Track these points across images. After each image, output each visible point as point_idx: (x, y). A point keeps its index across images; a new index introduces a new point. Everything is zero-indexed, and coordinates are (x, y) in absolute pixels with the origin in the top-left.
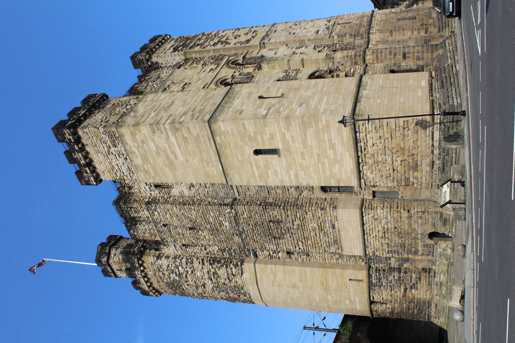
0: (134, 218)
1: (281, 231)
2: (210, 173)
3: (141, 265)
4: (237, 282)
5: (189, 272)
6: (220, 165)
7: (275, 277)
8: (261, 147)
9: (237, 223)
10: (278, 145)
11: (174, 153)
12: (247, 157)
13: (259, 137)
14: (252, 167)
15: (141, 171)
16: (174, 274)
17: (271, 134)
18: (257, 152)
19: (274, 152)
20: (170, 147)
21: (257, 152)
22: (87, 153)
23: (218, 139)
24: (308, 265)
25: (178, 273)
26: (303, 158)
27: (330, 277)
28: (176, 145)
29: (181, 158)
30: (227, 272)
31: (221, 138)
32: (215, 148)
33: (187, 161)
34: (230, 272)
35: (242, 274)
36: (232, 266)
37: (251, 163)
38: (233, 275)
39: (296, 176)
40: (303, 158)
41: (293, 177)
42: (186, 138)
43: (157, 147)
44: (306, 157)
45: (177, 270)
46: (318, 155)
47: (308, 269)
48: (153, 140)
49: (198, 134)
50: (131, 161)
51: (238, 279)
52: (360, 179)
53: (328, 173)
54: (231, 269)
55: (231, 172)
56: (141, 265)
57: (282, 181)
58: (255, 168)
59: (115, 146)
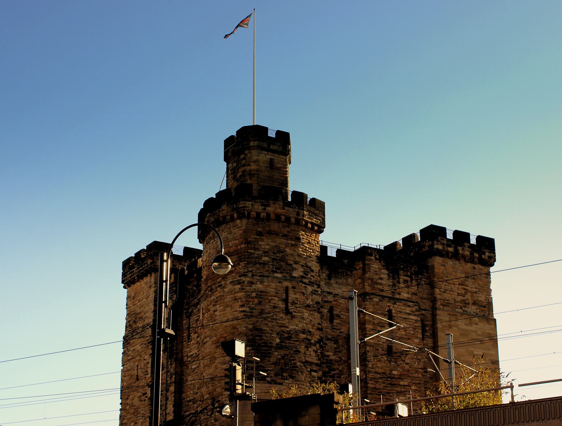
0: (398, 275)
4: (302, 372)
16: (302, 274)
25: (304, 280)
34: (315, 368)
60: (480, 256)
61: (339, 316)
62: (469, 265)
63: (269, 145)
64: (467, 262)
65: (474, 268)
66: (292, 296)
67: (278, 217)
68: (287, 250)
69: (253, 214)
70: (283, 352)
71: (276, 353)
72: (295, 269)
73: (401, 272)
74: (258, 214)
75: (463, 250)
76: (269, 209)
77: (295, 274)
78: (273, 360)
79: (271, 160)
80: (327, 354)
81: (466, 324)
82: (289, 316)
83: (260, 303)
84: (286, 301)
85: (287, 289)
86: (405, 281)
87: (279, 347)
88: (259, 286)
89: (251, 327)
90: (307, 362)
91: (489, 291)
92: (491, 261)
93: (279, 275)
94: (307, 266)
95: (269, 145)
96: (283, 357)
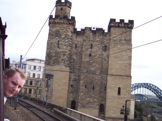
0: (96, 34)
1: (89, 88)
2: (113, 70)
3: (69, 23)
4: (61, 63)
5: (65, 44)
6: (115, 74)
7: (64, 79)
8: (121, 90)
9: (93, 73)
10: (122, 95)
11: (121, 60)
12: (118, 85)
13: (125, 90)
14: (115, 85)
15: (115, 45)
16: (64, 37)
17: (126, 94)
18: (119, 88)
19: (119, 93)
20: (123, 60)
21: (119, 88)
22: (123, 28)
23: (125, 77)
24: (68, 92)
25: (65, 38)
26: (116, 102)
27: (63, 100)
28: (124, 62)
29: (119, 62)
30: (66, 60)
31: (125, 78)
32: (122, 75)
33: (118, 64)
34: (66, 61)
35: (65, 66)
36: (68, 62)
37: (116, 85)
38: (64, 62)
39: (110, 99)
40: (116, 102)
41: (110, 97)
42: (126, 67)
43: (124, 55)
44: (117, 103)
45: (66, 38)
46: (117, 107)
47: (67, 92)
48: (126, 55)
49: (127, 71)
50: (119, 43)
51: (63, 63)
52: (108, 118)
53: (111, 108)
54: (67, 62)
55: (112, 77)
56: (69, 23)
57: (108, 93)
58: (114, 86)
59: (125, 40)
61: (78, 47)
62: (124, 29)
63: (61, 4)
65: (126, 30)
66: (60, 43)
67: (58, 22)
68: (61, 31)
69: (52, 23)
70: (56, 58)
74: (53, 23)
75: (121, 25)
76: (55, 21)
78: (52, 60)
79: (62, 8)
80: (73, 57)
81: (120, 46)
82: (59, 48)
83: (51, 46)
84: (58, 44)
85: (59, 41)
87: (54, 56)
88: (52, 41)
89: (48, 51)
90: (63, 60)
91: (131, 37)
92: (132, 28)
93: (57, 38)
94: (67, 34)
95: (61, 4)
96: (55, 59)
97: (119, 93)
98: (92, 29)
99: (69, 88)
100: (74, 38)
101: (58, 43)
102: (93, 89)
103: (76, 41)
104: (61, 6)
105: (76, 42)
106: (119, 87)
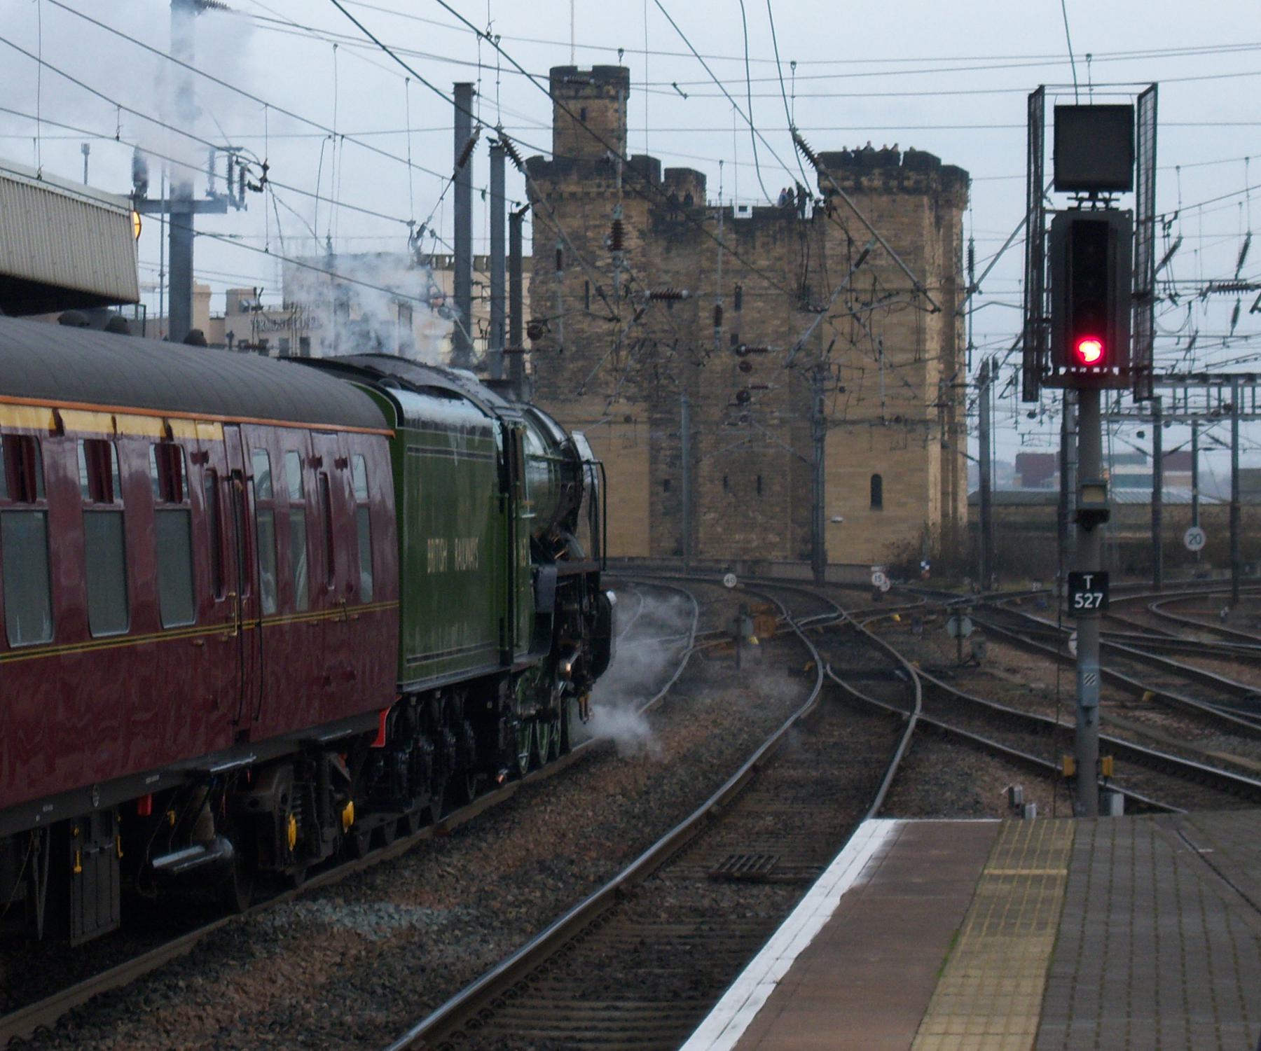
10: (889, 510)
18: (876, 481)
19: (876, 499)
21: (876, 481)
24: (652, 513)
60: (901, 183)
63: (577, 91)
64: (880, 195)
67: (573, 195)
68: (590, 234)
71: (571, 366)
72: (599, 256)
73: (758, 233)
75: (871, 180)
77: (599, 263)
82: (589, 319)
86: (764, 245)
87: (573, 358)
93: (578, 269)
95: (577, 91)
96: (580, 370)
97: (876, 499)
98: (738, 215)
99: (652, 494)
100: (658, 261)
101: (582, 293)
102: (759, 490)
103: (666, 272)
104: (575, 98)
105: (667, 278)
106: (875, 472)
